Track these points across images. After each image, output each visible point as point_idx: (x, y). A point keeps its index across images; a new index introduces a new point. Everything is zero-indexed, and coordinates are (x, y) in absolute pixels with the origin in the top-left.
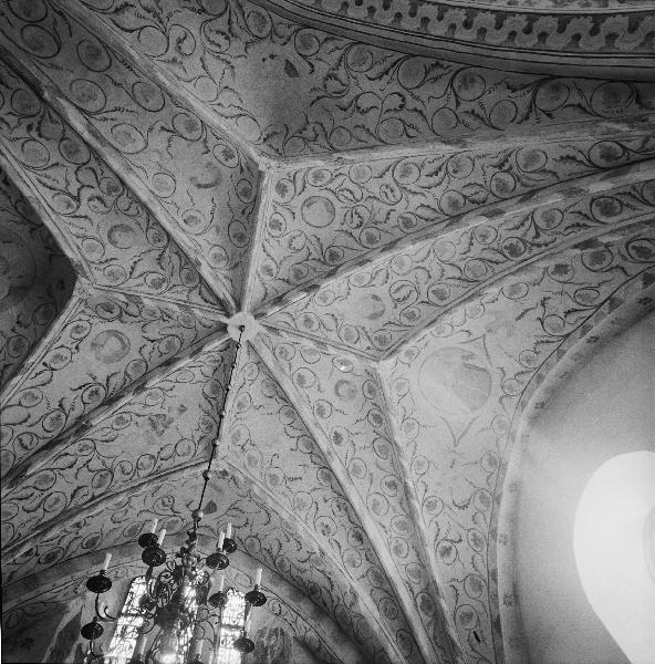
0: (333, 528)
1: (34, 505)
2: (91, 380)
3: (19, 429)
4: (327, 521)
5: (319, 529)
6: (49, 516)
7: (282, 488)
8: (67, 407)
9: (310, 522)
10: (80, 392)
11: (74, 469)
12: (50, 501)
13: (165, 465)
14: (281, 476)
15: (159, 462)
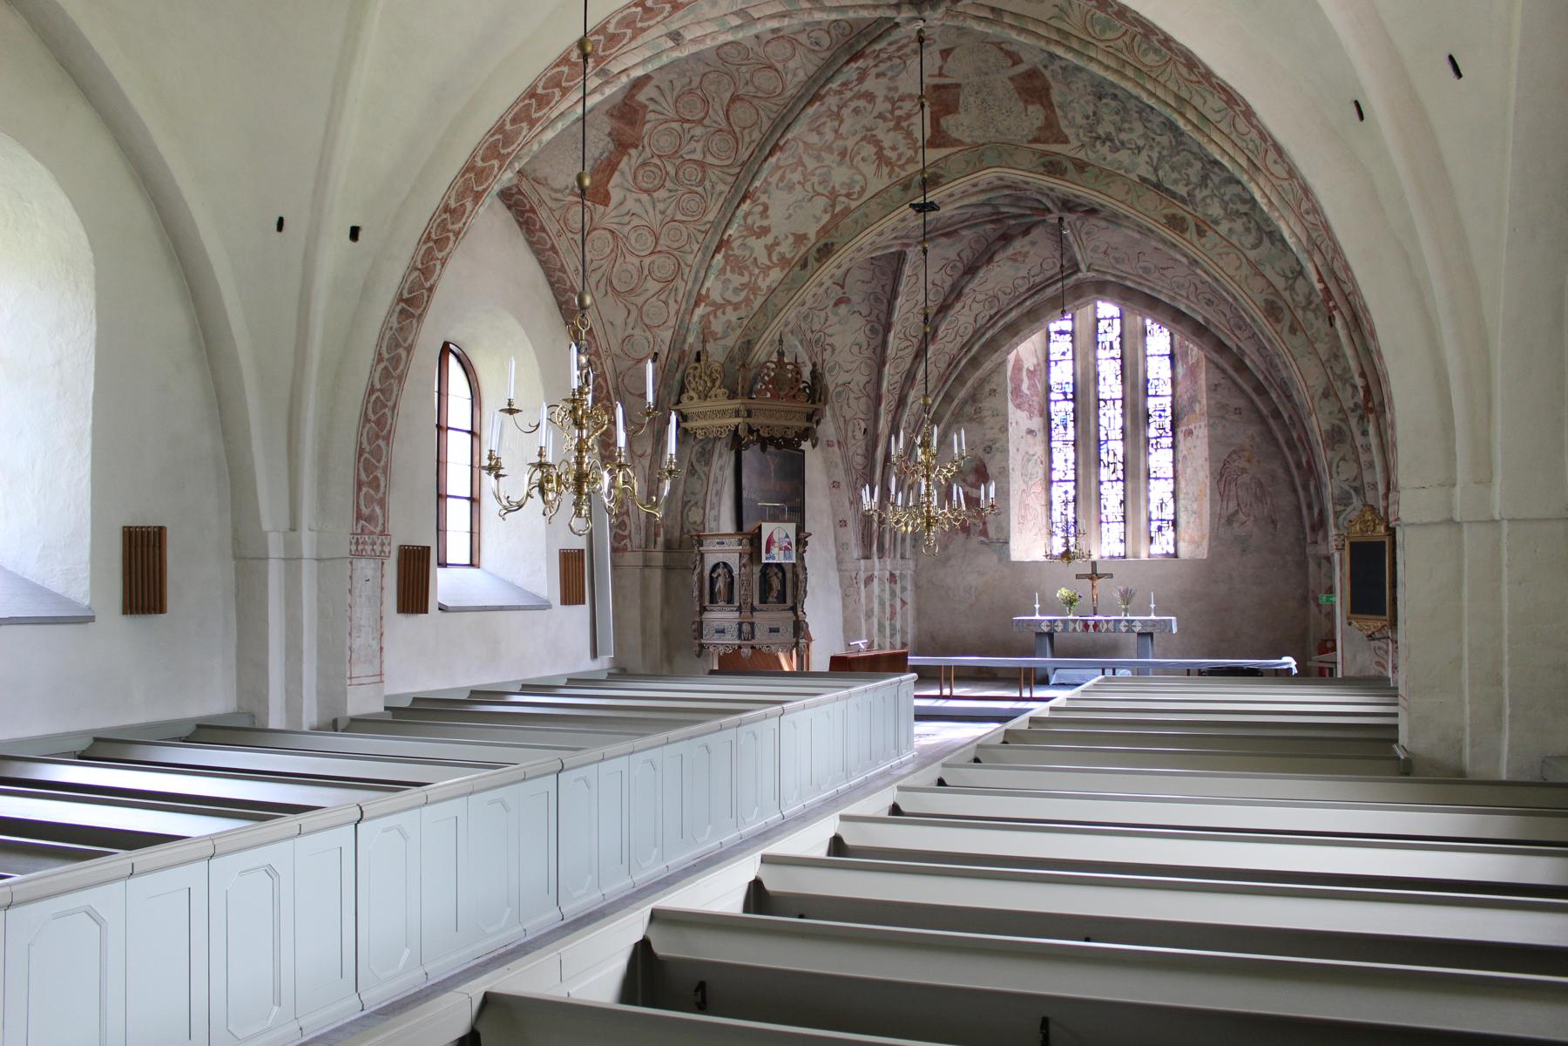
0: (1216, 301)
1: (953, 335)
2: (944, 262)
3: (915, 311)
4: (1208, 296)
5: (1204, 301)
6: (965, 339)
7: (1157, 275)
8: (939, 283)
9: (1195, 301)
10: (943, 271)
11: (967, 308)
12: (961, 332)
13: (1038, 279)
14: (1152, 267)
15: (1032, 279)
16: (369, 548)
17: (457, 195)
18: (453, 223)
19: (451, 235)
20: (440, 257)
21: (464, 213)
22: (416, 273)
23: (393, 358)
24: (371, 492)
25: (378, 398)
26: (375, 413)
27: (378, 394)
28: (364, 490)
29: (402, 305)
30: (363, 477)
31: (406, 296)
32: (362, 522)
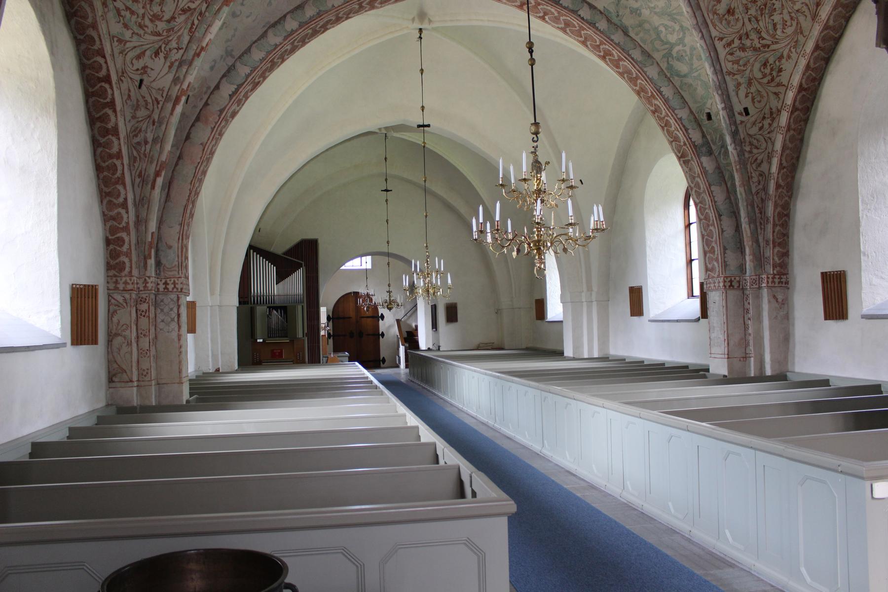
16: (712, 285)
17: (649, 104)
18: (661, 114)
19: (666, 118)
20: (674, 129)
21: (659, 107)
22: (674, 143)
23: (695, 185)
24: (711, 255)
25: (700, 207)
26: (702, 215)
27: (700, 205)
28: (708, 255)
29: (681, 159)
30: (706, 248)
31: (679, 155)
32: (709, 272)
